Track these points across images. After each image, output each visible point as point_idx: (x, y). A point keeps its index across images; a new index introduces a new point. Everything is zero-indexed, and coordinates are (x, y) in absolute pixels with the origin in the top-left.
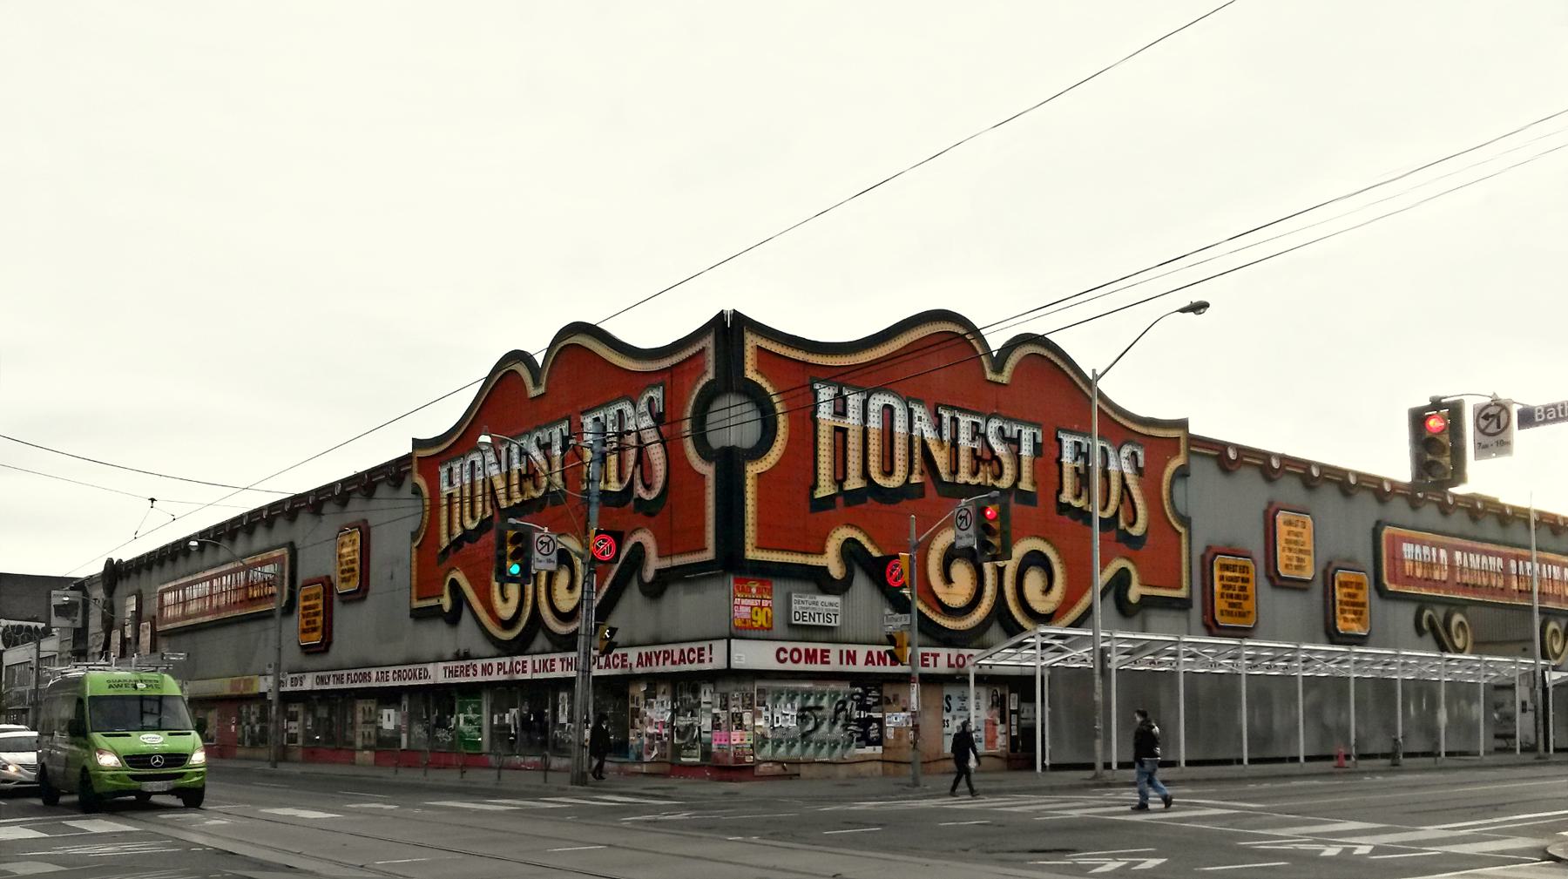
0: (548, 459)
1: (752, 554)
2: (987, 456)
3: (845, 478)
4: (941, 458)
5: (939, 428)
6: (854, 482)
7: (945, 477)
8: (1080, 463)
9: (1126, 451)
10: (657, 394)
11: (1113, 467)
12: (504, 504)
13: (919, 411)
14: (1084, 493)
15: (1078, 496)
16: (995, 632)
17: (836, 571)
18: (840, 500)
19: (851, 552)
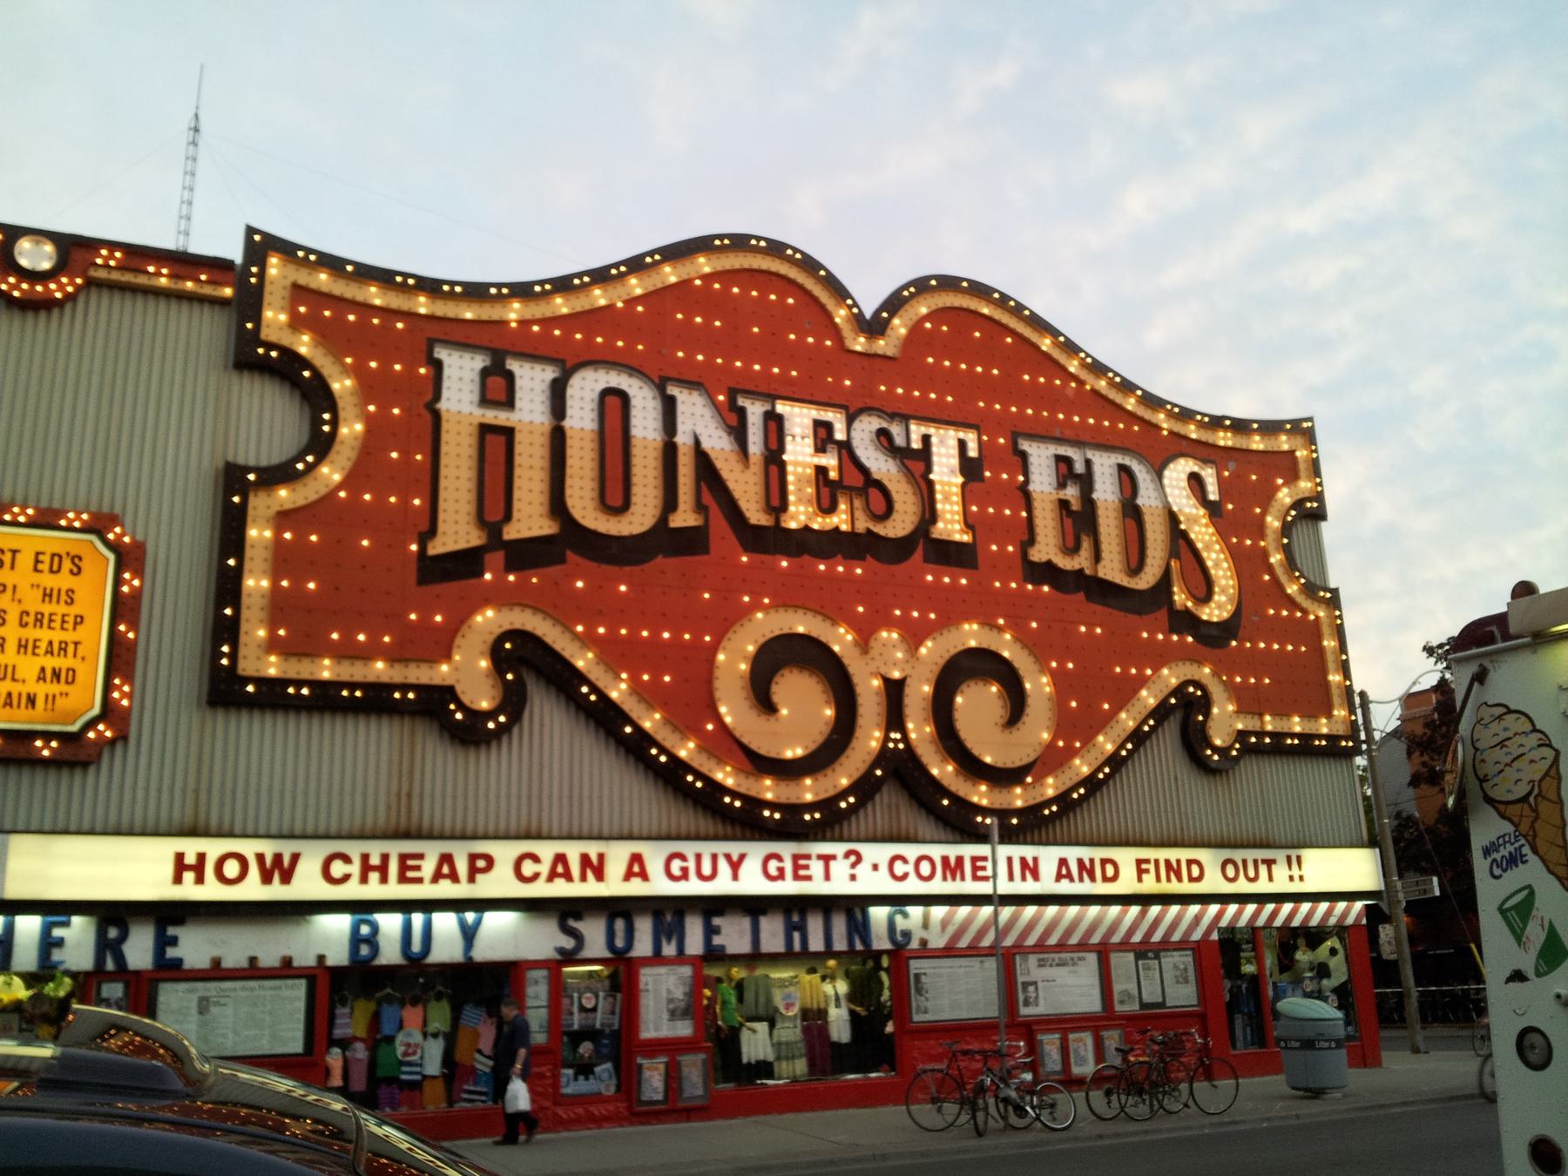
2: (858, 481)
3: (508, 517)
4: (746, 487)
5: (738, 432)
7: (756, 515)
8: (1071, 492)
9: (1178, 471)
11: (1147, 498)
14: (1086, 544)
15: (1072, 550)
18: (498, 557)
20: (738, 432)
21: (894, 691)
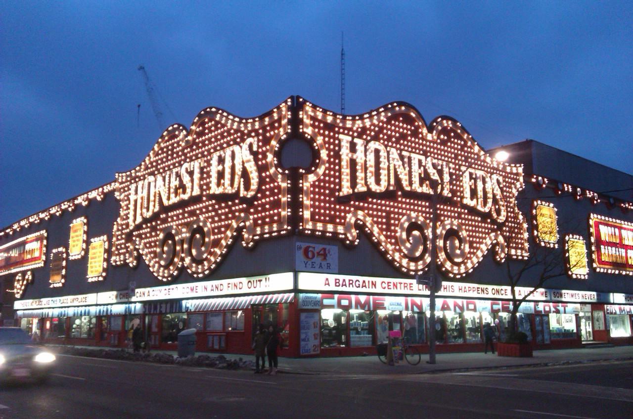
0: (192, 181)
6: (361, 188)
9: (495, 177)
15: (472, 199)
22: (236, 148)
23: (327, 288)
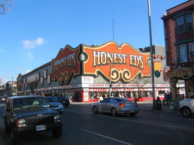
1: (84, 73)
2: (118, 59)
4: (111, 59)
5: (111, 56)
9: (140, 57)
10: (74, 53)
11: (138, 59)
12: (60, 67)
13: (108, 53)
15: (132, 63)
16: (120, 82)
17: (96, 75)
18: (97, 66)
19: (99, 73)
20: (111, 56)
21: (121, 74)
22: (72, 55)
23: (90, 87)
